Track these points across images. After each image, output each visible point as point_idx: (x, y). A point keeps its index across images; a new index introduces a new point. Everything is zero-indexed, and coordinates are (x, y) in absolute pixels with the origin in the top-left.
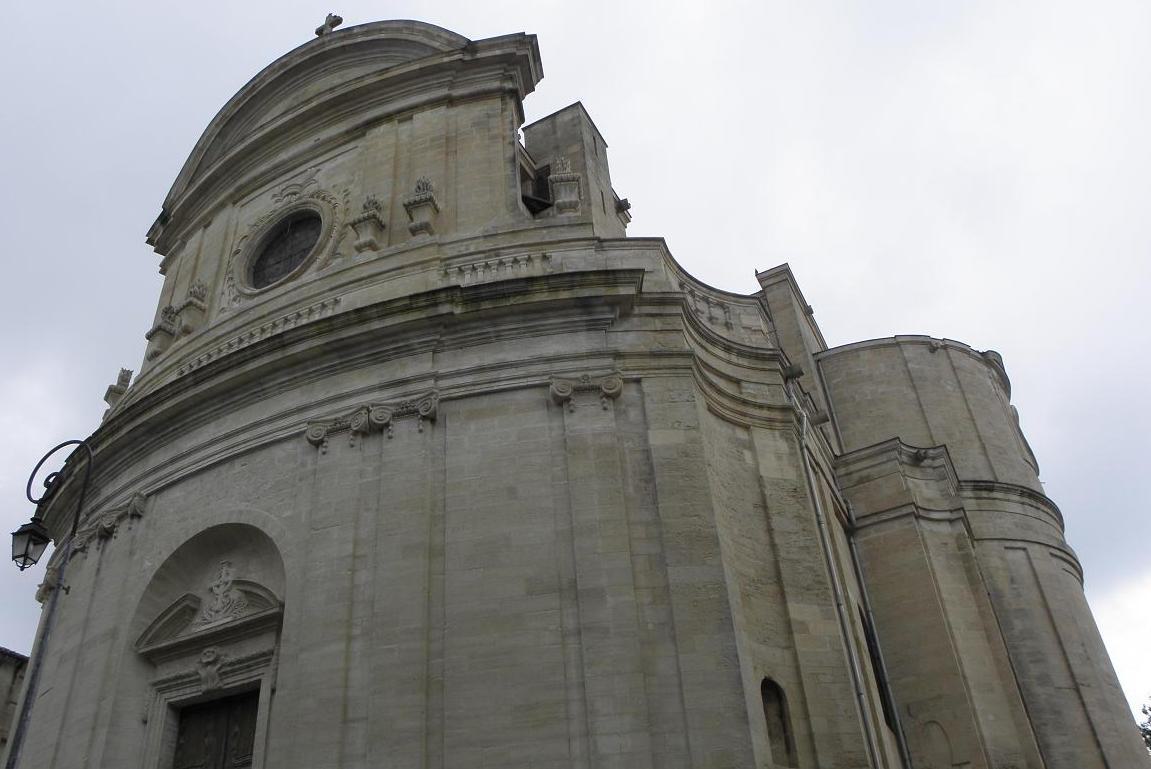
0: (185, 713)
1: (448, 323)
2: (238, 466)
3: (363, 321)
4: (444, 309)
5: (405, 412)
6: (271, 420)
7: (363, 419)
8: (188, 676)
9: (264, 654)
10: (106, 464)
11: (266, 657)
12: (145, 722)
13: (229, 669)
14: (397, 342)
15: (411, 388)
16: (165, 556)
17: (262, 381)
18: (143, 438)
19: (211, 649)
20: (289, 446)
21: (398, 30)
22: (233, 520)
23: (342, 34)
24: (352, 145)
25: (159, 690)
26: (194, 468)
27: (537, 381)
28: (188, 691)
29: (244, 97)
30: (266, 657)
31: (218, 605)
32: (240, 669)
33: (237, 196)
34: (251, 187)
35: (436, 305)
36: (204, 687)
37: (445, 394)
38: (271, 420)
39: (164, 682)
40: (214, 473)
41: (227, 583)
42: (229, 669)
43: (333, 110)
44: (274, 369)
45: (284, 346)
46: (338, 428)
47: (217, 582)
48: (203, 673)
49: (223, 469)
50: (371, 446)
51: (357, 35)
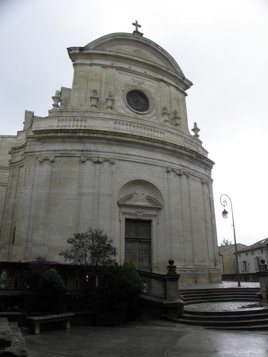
0: (127, 220)
1: (191, 157)
2: (146, 166)
3: (181, 149)
4: (194, 155)
5: (185, 174)
6: (157, 160)
7: (178, 173)
8: (133, 213)
9: (154, 215)
10: (93, 139)
11: (155, 216)
12: (120, 221)
13: (145, 215)
14: (183, 156)
15: (185, 168)
16: (127, 181)
17: (155, 148)
18: (114, 141)
19: (141, 209)
20: (160, 168)
21: (169, 57)
22: (148, 181)
23: (156, 45)
24: (154, 81)
25: (123, 214)
26: (134, 160)
27: (200, 177)
28: (132, 216)
29: (122, 36)
30: (155, 216)
31: (139, 199)
32: (147, 216)
33: (119, 69)
34: (124, 70)
35: (193, 154)
36: (138, 218)
37: (191, 173)
38: (157, 160)
39: (125, 212)
40: (139, 164)
41: (141, 194)
42: (145, 215)
43: (153, 68)
44: (159, 147)
45: (164, 144)
46: (173, 170)
47: (138, 192)
48: (138, 214)
49: (143, 164)
50: (178, 178)
51: (159, 49)
